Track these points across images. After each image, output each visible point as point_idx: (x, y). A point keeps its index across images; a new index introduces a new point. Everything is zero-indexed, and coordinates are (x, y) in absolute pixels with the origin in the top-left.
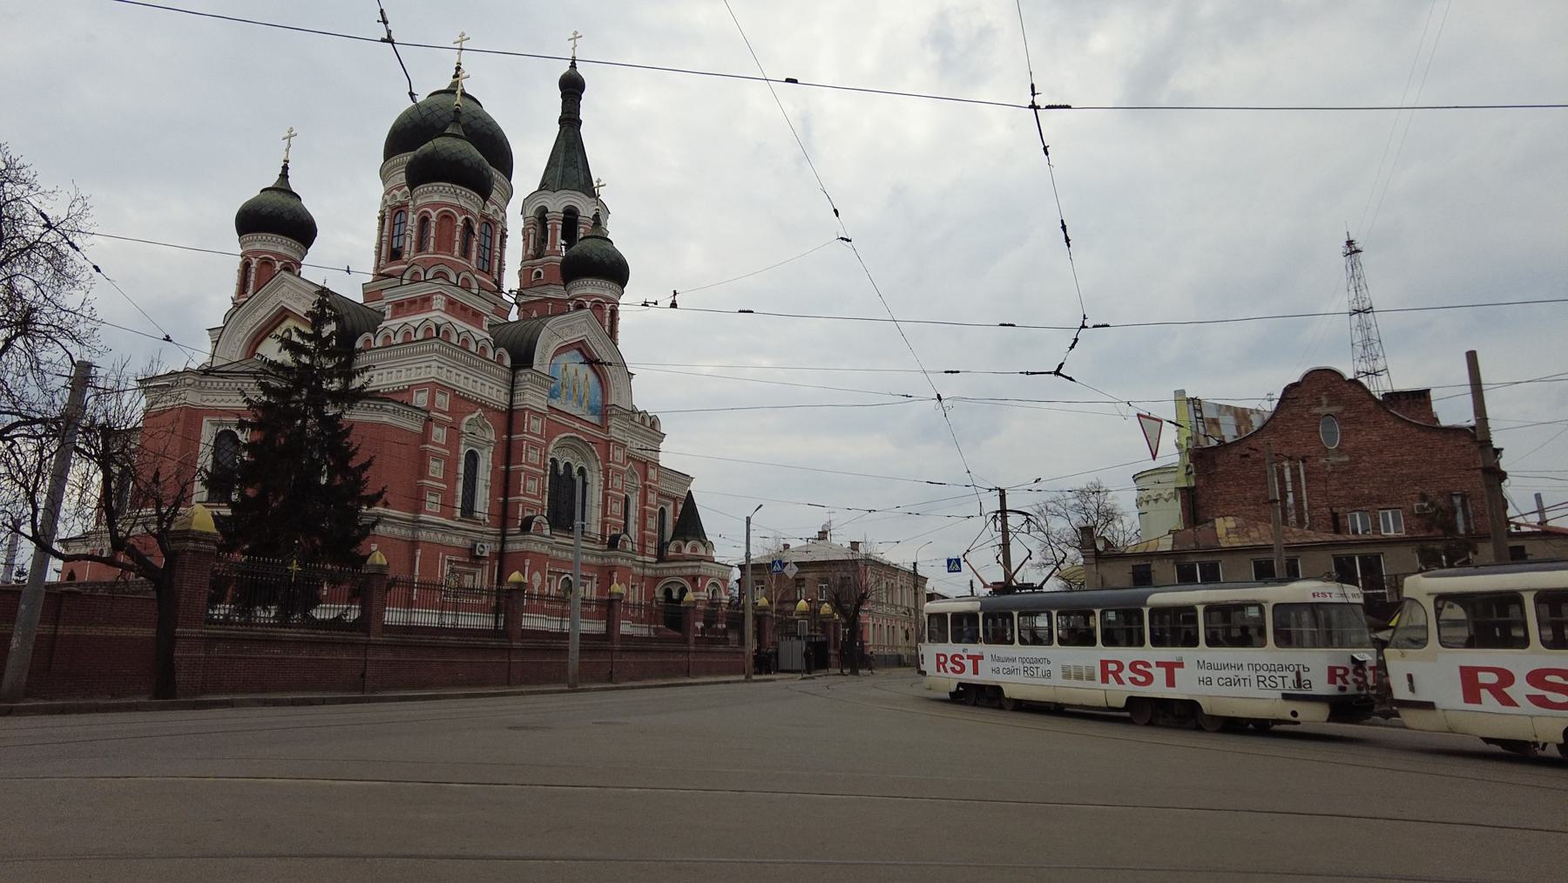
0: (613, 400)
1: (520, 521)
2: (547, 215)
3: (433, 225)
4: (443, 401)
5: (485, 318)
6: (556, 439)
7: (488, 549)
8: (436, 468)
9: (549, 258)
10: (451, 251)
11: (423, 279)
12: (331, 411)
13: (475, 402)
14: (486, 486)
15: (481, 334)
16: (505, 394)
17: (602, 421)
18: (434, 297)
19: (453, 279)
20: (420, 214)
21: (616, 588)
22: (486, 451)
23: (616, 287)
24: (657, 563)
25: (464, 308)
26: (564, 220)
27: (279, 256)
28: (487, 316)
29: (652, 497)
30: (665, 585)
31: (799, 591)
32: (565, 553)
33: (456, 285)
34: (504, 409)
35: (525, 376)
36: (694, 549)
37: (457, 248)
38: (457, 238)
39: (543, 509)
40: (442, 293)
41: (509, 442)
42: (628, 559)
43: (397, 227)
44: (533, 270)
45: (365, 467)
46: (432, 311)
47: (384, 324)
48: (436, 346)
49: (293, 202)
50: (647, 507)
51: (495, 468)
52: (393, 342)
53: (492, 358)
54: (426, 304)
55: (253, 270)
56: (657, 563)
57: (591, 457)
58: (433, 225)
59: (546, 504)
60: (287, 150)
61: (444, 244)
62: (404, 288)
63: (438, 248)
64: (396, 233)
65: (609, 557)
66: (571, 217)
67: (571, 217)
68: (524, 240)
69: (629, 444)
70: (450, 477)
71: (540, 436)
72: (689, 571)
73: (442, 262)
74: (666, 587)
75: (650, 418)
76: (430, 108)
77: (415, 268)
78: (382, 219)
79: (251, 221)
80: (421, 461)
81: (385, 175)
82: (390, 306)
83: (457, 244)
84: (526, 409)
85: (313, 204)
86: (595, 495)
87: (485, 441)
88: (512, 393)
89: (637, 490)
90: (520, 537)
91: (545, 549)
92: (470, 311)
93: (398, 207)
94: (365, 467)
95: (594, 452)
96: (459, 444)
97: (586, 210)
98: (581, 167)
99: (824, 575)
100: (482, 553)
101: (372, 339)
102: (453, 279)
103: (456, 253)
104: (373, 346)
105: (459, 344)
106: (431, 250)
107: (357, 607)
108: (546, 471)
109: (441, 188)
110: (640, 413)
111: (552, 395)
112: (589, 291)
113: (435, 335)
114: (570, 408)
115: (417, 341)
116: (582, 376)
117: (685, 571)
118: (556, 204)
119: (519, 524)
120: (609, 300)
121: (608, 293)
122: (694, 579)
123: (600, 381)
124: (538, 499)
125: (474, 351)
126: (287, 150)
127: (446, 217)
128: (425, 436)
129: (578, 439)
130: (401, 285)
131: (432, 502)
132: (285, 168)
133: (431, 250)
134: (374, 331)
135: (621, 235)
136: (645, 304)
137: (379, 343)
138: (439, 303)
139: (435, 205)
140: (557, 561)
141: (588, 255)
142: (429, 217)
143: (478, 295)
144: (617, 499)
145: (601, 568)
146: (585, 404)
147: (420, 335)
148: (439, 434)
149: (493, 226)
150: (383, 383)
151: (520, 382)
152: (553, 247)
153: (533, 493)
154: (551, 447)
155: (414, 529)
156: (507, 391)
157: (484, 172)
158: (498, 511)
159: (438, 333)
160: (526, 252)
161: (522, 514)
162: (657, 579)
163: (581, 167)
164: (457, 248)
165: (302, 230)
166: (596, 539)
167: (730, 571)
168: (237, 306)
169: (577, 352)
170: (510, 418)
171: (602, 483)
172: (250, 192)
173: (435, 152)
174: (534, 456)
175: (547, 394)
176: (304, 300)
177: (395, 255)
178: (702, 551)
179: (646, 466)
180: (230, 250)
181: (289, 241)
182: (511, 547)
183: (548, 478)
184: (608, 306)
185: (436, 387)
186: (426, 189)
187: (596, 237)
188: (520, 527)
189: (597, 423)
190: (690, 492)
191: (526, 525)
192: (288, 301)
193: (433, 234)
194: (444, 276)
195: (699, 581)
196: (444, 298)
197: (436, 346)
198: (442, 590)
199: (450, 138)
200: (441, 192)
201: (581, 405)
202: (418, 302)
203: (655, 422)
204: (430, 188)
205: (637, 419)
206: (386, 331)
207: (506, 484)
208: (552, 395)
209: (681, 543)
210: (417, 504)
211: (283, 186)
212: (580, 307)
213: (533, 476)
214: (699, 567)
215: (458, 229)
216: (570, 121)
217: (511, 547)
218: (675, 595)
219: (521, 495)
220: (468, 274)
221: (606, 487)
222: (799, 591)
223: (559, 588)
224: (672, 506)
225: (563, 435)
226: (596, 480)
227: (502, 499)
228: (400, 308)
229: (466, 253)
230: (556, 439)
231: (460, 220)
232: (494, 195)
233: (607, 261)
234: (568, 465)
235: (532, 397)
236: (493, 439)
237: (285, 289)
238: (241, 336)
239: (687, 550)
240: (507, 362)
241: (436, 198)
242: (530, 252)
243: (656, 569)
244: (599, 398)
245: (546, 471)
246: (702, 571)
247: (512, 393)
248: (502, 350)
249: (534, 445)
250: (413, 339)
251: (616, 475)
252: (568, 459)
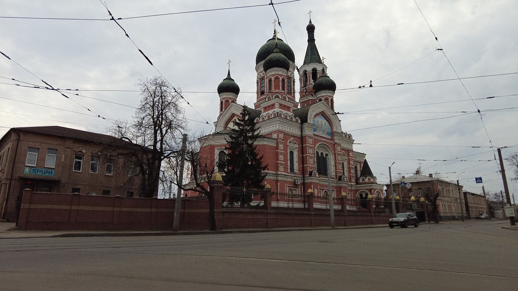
0: (335, 130)
1: (308, 172)
2: (307, 72)
3: (273, 81)
4: (281, 136)
5: (291, 108)
6: (317, 145)
7: (299, 182)
8: (281, 157)
9: (309, 86)
10: (279, 89)
11: (272, 99)
12: (250, 142)
13: (291, 135)
14: (297, 162)
15: (291, 114)
17: (332, 137)
18: (276, 104)
19: (281, 97)
20: (269, 79)
21: (344, 194)
22: (296, 151)
23: (332, 92)
24: (356, 185)
25: (285, 106)
26: (312, 73)
27: (230, 99)
28: (292, 108)
29: (352, 162)
30: (359, 193)
31: (410, 193)
32: (324, 183)
33: (282, 99)
34: (300, 137)
35: (305, 125)
36: (369, 179)
37: (281, 88)
38: (281, 84)
39: (315, 168)
40: (277, 102)
41: (302, 147)
42: (346, 184)
43: (262, 84)
44: (304, 91)
45: (261, 158)
46: (275, 108)
47: (262, 114)
48: (278, 119)
49: (232, 81)
50: (350, 166)
51: (299, 156)
52: (265, 119)
53: (294, 121)
54: (273, 106)
55: (224, 104)
56: (356, 185)
57: (328, 149)
58: (273, 81)
59: (316, 166)
60: (229, 67)
61: (277, 87)
62: (266, 103)
63: (275, 88)
64: (262, 86)
65: (339, 183)
66: (314, 71)
67: (314, 71)
68: (300, 82)
69: (342, 144)
70: (285, 160)
71: (312, 144)
72: (368, 188)
73: (277, 93)
74: (361, 193)
75: (348, 135)
76: (268, 45)
77: (269, 96)
78: (258, 83)
79: (222, 89)
80: (277, 154)
81: (257, 69)
82: (263, 109)
83: (281, 86)
84: (307, 136)
85: (237, 82)
87: (295, 147)
88: (302, 131)
89: (346, 160)
90: (309, 178)
91: (317, 181)
92: (287, 107)
93: (262, 78)
94: (261, 158)
96: (287, 149)
97: (319, 68)
98: (316, 54)
100: (298, 183)
101: (259, 119)
102: (281, 97)
103: (281, 89)
104: (259, 121)
105: (284, 118)
106: (273, 89)
107: (263, 201)
108: (315, 155)
109: (274, 70)
110: (344, 134)
111: (314, 131)
112: (323, 94)
113: (277, 116)
114: (320, 133)
115: (272, 118)
116: (323, 123)
117: (366, 188)
118: (309, 68)
119: (308, 173)
120: (330, 96)
121: (329, 94)
122: (370, 190)
123: (330, 124)
124: (314, 165)
125: (289, 119)
126: (229, 67)
127: (277, 78)
128: (277, 148)
129: (324, 144)
130: (266, 102)
131: (281, 168)
132: (229, 72)
133: (273, 89)
134: (259, 117)
135: (332, 74)
136: (360, 87)
137: (261, 120)
138: (277, 105)
139: (273, 75)
140: (321, 185)
141: (322, 82)
142: (271, 79)
143: (288, 101)
144: (339, 163)
145: (337, 187)
146: (325, 132)
147: (273, 116)
148: (281, 146)
149: (290, 79)
150: (263, 132)
151: (304, 127)
152: (310, 82)
153: (312, 164)
154: (316, 148)
155: (277, 177)
156: (300, 131)
157: (287, 62)
158: (301, 169)
159: (278, 115)
160: (301, 86)
161: (309, 170)
162: (356, 191)
163: (316, 54)
164: (281, 88)
165: (235, 90)
166: (334, 177)
168: (221, 115)
169: (321, 115)
170: (302, 139)
171: (334, 158)
172: (221, 81)
173: (271, 59)
174: (311, 151)
175: (313, 130)
176: (238, 110)
177: (262, 93)
178: (372, 180)
179: (349, 151)
180: (217, 99)
181: (232, 93)
182: (306, 181)
183: (316, 158)
184: (330, 99)
185: (278, 132)
186: (270, 71)
187: (324, 76)
188: (309, 174)
189: (330, 138)
190: (365, 159)
191: (311, 174)
192: (234, 111)
193: (273, 84)
194: (278, 97)
195: (372, 191)
196: (278, 104)
197: (278, 119)
198: (286, 195)
199: (275, 53)
200: (274, 71)
201: (324, 133)
202: (271, 106)
203: (350, 136)
204: (271, 70)
205: (344, 135)
206: (263, 116)
207: (303, 160)
208: (314, 131)
209: (364, 178)
210: (277, 169)
211: (229, 78)
212: (320, 100)
213: (311, 157)
214: (372, 186)
215: (281, 82)
216: (311, 40)
217: (306, 181)
218: (364, 196)
219: (308, 164)
220: (285, 95)
221: (335, 160)
222: (410, 193)
223: (323, 194)
224: (359, 165)
226: (332, 158)
227: (302, 166)
228: (266, 109)
229: (283, 89)
230: (317, 145)
231: (281, 78)
232: (290, 69)
233: (328, 84)
234: (322, 153)
235: (308, 132)
236: (297, 147)
237: (233, 108)
238: (222, 123)
239: (366, 180)
240: (299, 122)
241: (273, 73)
242: (302, 86)
243: (356, 187)
244: (330, 130)
245: (315, 155)
247: (302, 131)
248: (297, 118)
249: (310, 148)
250: (271, 118)
251: (338, 155)
252: (322, 151)
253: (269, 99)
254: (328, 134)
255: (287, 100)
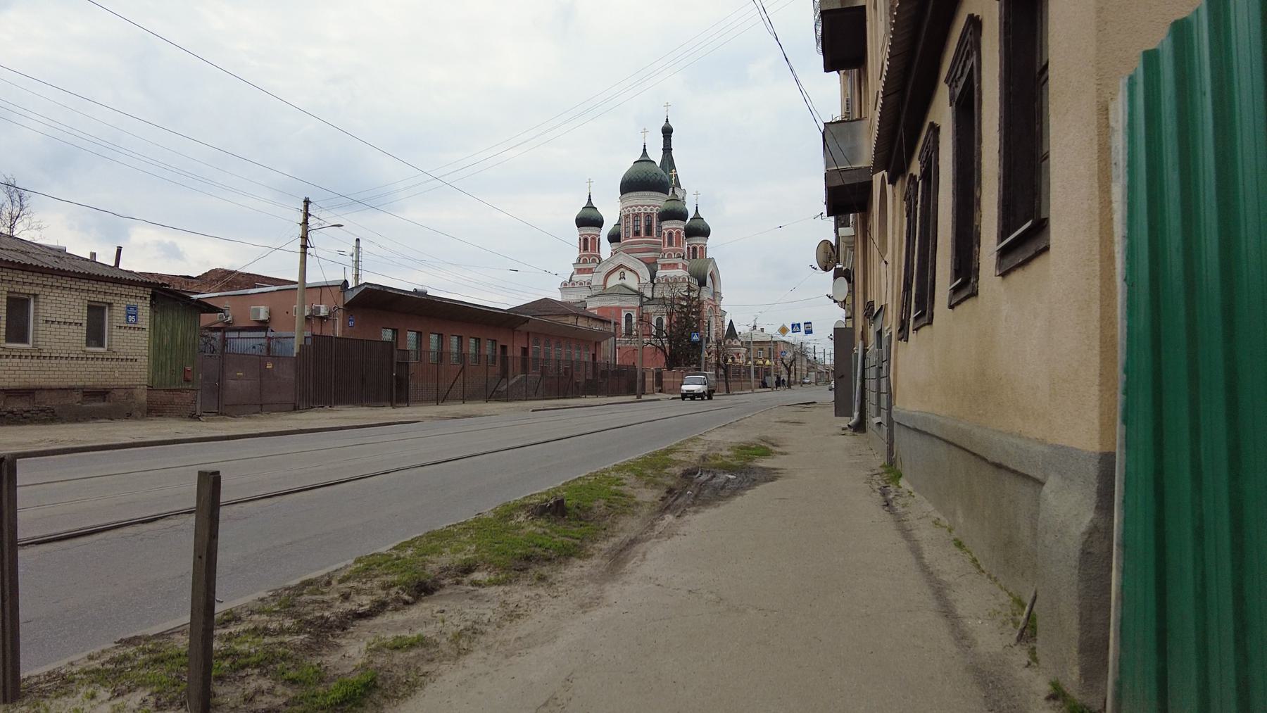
35: (703, 288)
36: (735, 343)
99: (761, 347)
112: (698, 242)
127: (678, 233)
138: (680, 266)
165: (598, 223)
180: (575, 234)
211: (590, 206)
216: (667, 149)
241: (674, 226)
253: (670, 256)
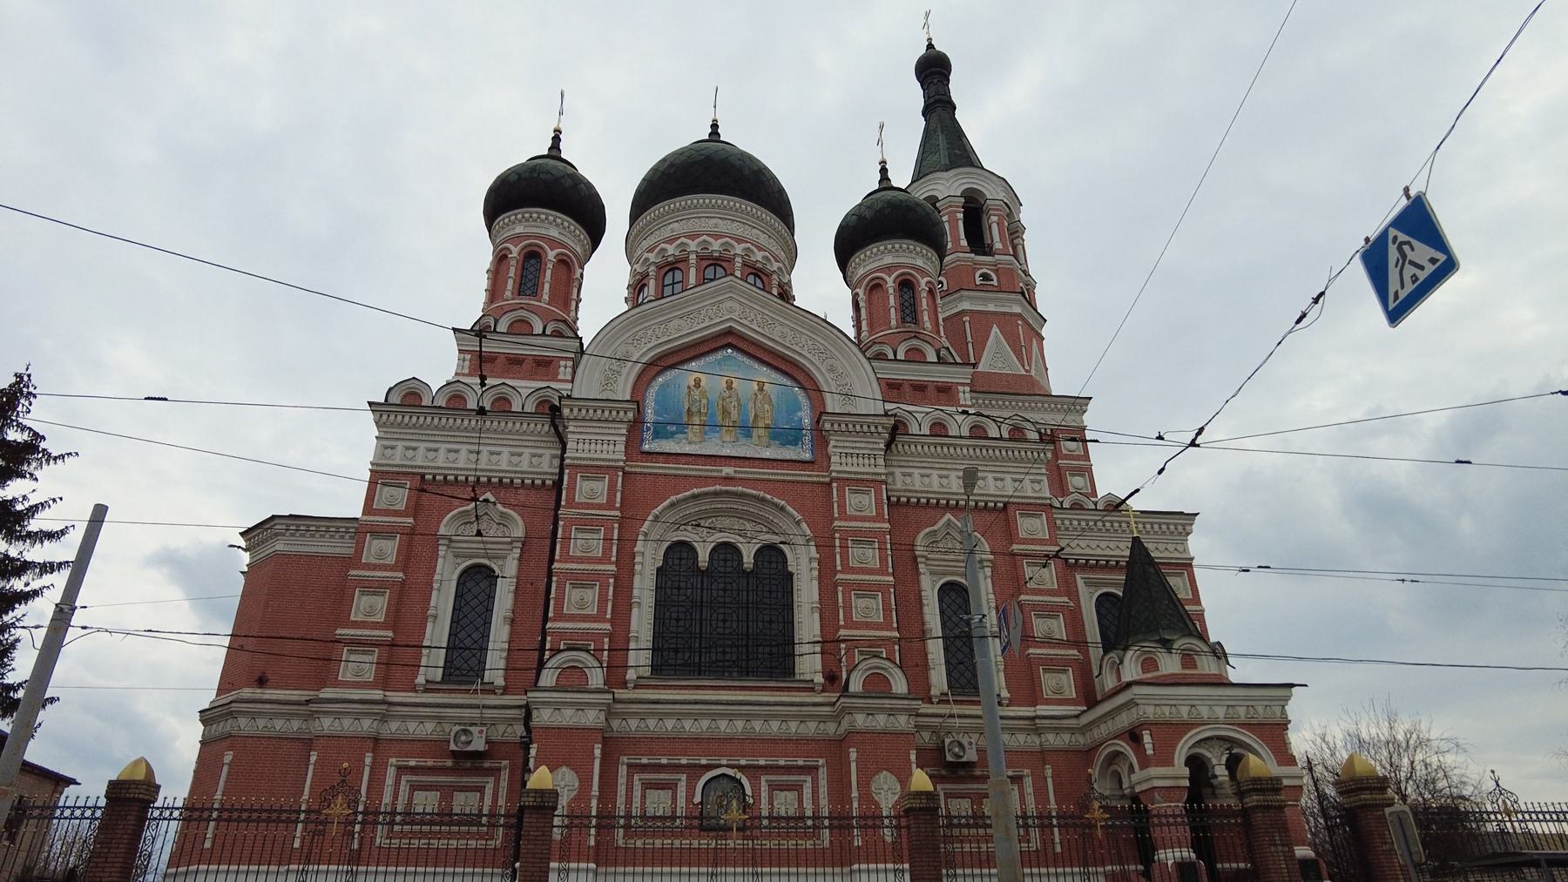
16: (554, 457)
21: (541, 778)
38: (512, 274)
72: (1124, 721)
86: (807, 592)
95: (782, 509)
116: (745, 389)
167: (1288, 698)
171: (815, 565)
178: (1207, 666)
195: (1147, 738)
225: (673, 498)
246: (1150, 712)
254: (790, 436)
255: (538, 329)
